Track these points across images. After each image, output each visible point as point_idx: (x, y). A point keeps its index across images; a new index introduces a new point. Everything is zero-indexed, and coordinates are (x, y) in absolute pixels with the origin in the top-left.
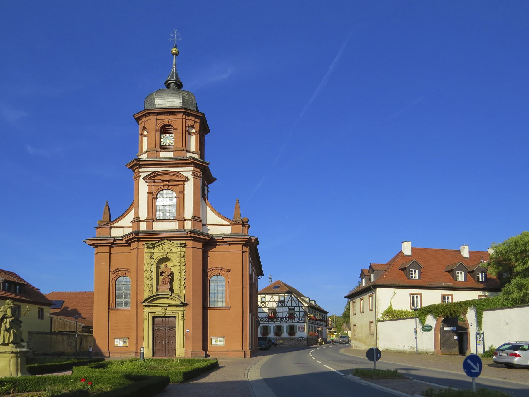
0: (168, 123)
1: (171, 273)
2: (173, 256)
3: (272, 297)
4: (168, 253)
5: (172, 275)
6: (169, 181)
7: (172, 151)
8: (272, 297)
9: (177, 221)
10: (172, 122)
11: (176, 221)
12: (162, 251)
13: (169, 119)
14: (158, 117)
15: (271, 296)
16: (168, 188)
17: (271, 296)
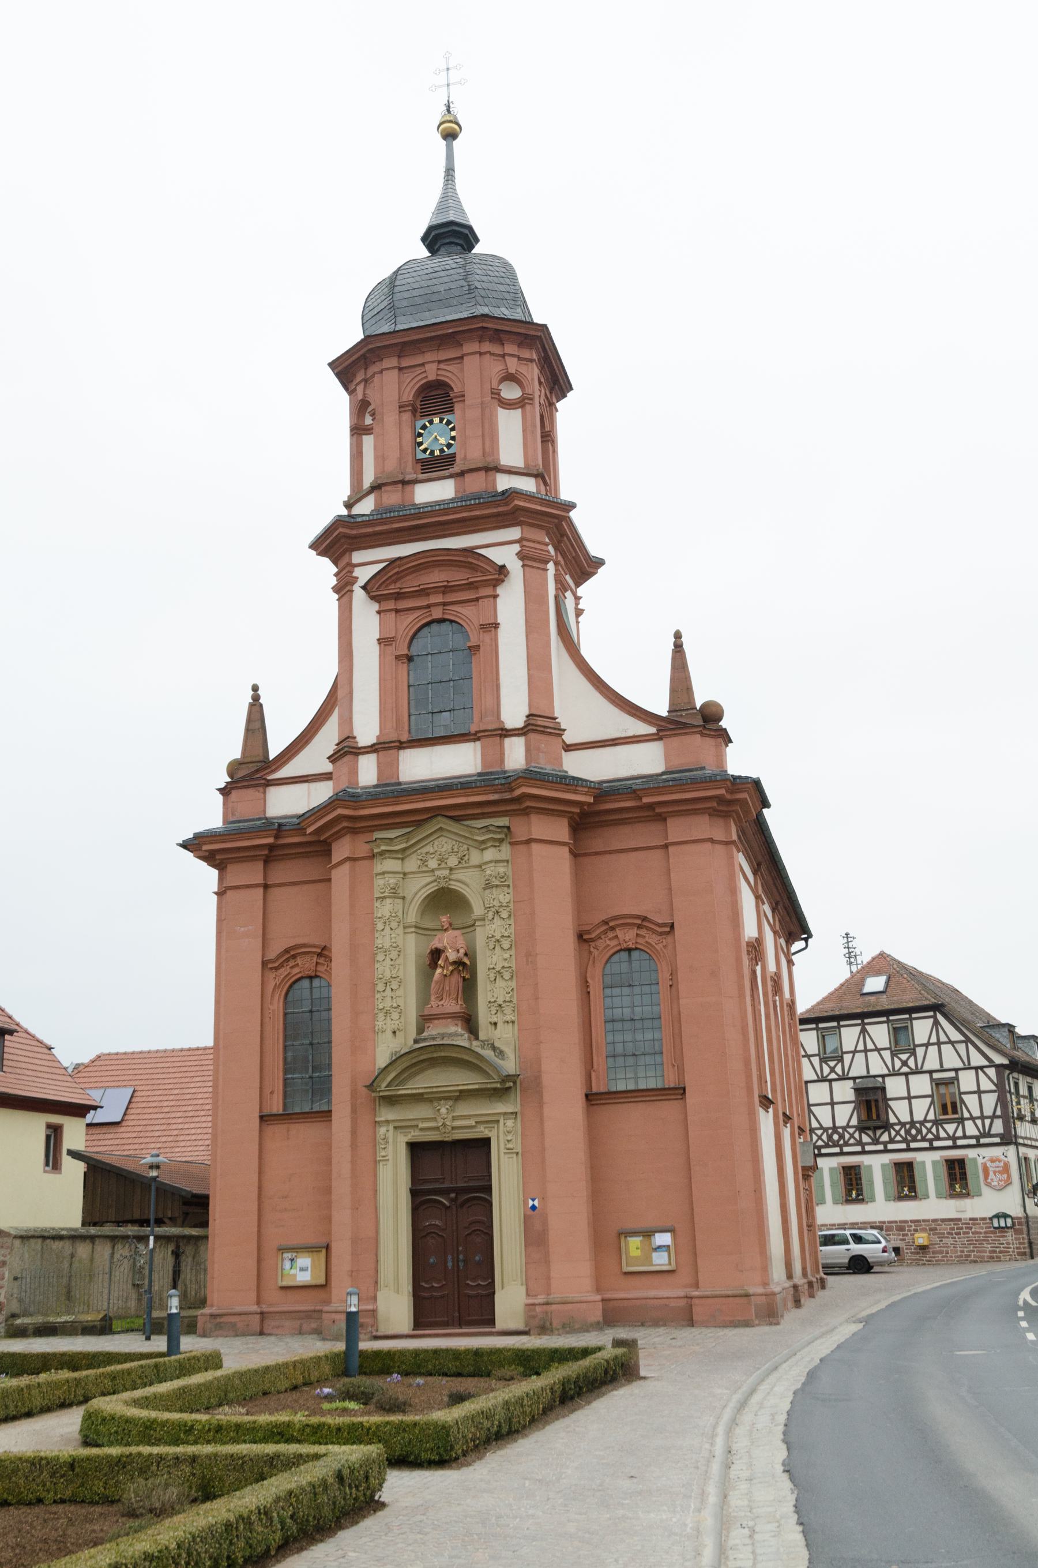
0: (437, 375)
1: (466, 954)
2: (467, 880)
3: (864, 1031)
4: (451, 869)
5: (468, 962)
6: (447, 589)
7: (451, 476)
8: (864, 1031)
9: (478, 739)
10: (450, 374)
11: (474, 740)
12: (433, 864)
13: (439, 362)
14: (406, 362)
15: (859, 1028)
16: (444, 613)
17: (859, 1028)
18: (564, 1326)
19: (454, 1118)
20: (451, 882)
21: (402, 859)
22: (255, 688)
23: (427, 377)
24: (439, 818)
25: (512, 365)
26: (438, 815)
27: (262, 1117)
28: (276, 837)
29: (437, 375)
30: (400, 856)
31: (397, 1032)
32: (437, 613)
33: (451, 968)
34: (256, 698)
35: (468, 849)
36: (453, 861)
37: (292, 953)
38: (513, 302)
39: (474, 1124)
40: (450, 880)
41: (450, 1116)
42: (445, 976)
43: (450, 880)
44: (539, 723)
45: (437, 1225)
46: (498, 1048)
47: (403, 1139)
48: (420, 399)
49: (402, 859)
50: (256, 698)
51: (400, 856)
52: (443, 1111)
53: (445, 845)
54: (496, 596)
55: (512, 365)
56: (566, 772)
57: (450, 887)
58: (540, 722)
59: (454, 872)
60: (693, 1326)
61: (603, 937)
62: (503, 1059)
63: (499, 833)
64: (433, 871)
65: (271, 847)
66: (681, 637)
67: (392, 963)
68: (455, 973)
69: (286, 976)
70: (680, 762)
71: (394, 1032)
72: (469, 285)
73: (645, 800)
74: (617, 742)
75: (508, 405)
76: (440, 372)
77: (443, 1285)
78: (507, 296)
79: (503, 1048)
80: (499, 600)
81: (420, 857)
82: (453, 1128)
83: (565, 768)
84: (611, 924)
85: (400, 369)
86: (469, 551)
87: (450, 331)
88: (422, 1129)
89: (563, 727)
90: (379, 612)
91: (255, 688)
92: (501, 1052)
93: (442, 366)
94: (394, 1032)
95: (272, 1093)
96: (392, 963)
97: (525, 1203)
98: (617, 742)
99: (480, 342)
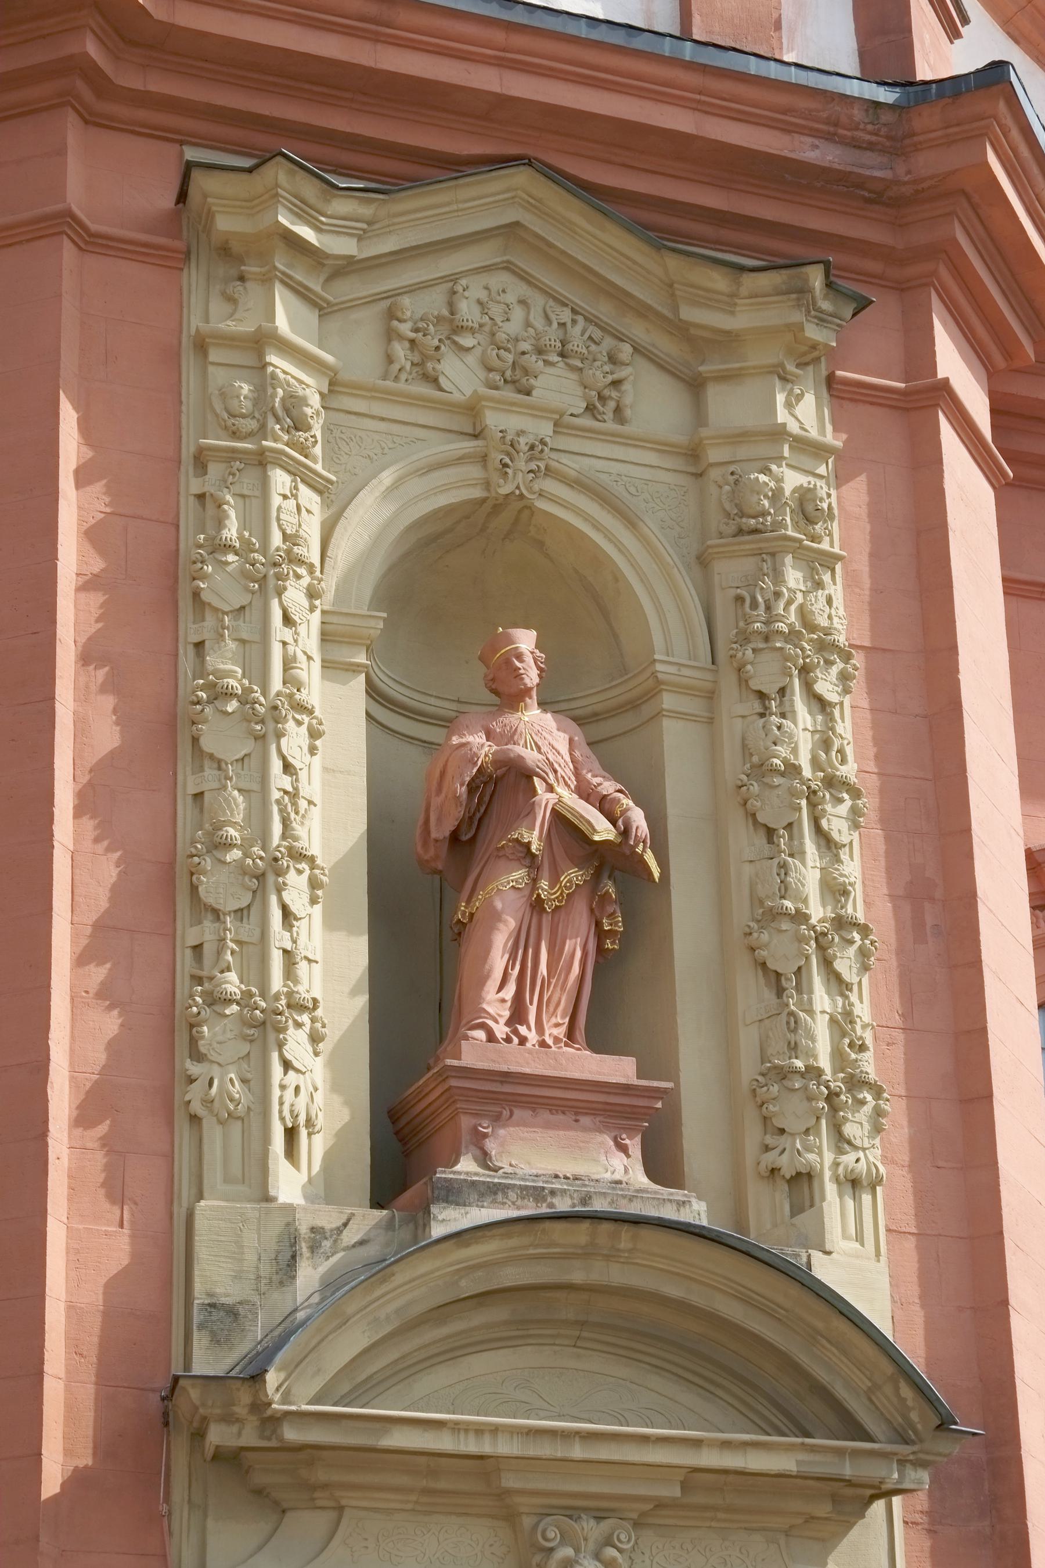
20: (550, 486)
24: (521, 178)
31: (303, 1132)
40: (549, 472)
43: (549, 472)
53: (518, 314)
57: (542, 505)
64: (472, 409)
71: (291, 1134)
94: (291, 1134)
96: (286, 782)
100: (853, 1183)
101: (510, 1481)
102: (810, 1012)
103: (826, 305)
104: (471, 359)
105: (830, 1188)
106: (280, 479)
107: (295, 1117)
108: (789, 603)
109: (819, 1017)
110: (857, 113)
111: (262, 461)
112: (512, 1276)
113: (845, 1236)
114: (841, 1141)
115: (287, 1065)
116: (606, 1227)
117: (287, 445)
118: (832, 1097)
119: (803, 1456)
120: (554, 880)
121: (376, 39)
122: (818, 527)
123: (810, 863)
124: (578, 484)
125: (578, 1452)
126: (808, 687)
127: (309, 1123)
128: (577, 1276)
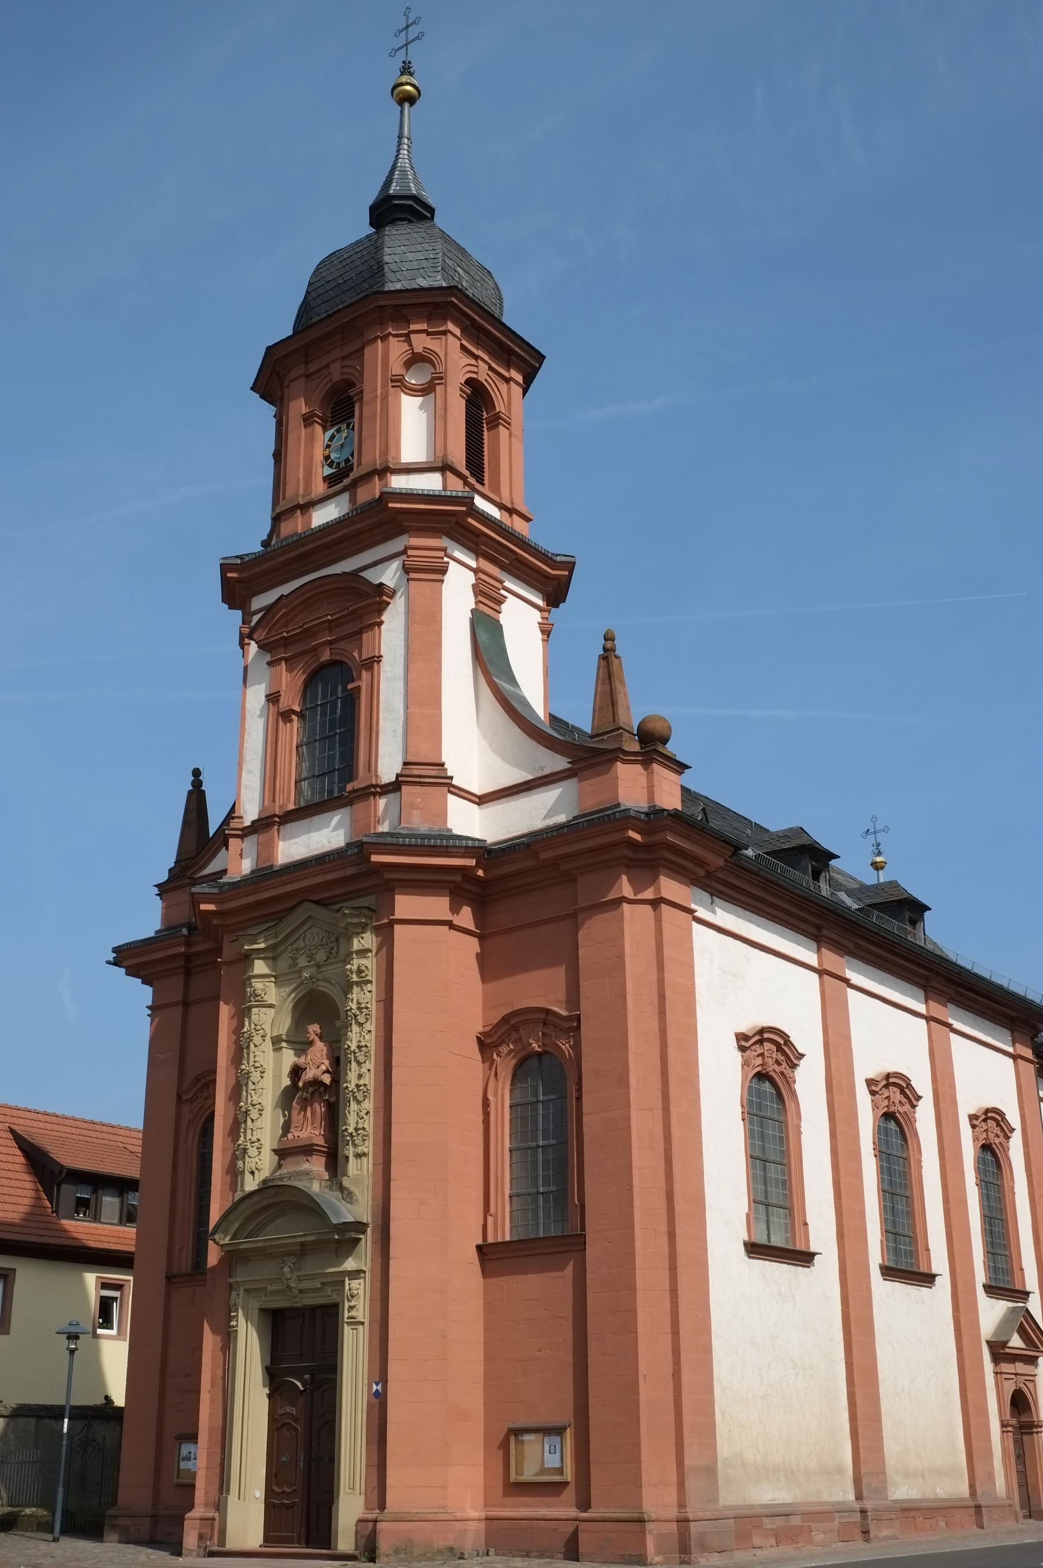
0: (342, 374)
13: (343, 358)
14: (313, 368)
18: (397, 1552)
19: (300, 1279)
20: (320, 983)
21: (274, 959)
22: (197, 773)
23: (331, 380)
25: (421, 342)
26: (303, 901)
27: (168, 1278)
28: (188, 944)
29: (342, 374)
30: (270, 955)
31: (256, 1172)
32: (326, 656)
33: (311, 1090)
34: (197, 784)
35: (337, 940)
36: (321, 956)
37: (203, 1081)
38: (432, 270)
39: (319, 1286)
40: (318, 980)
41: (294, 1276)
42: (306, 1099)
43: (318, 980)
44: (415, 772)
45: (292, 1414)
46: (347, 1189)
47: (255, 1305)
48: (331, 405)
49: (274, 959)
50: (197, 784)
51: (270, 955)
52: (286, 1270)
54: (381, 623)
55: (421, 342)
56: (450, 830)
57: (319, 988)
58: (416, 771)
59: (323, 969)
60: (578, 1560)
61: (506, 1040)
62: (351, 1203)
63: (358, 916)
65: (188, 958)
66: (613, 639)
67: (253, 1087)
68: (316, 1095)
69: (200, 1109)
70: (594, 802)
72: (378, 262)
73: (543, 856)
74: (531, 785)
75: (414, 391)
76: (344, 371)
77: (295, 1490)
78: (425, 264)
79: (352, 1188)
80: (383, 627)
81: (290, 955)
82: (301, 1291)
83: (449, 826)
84: (513, 1022)
85: (307, 377)
86: (355, 575)
87: (346, 320)
88: (271, 1293)
89: (449, 774)
90: (269, 664)
91: (197, 773)
92: (350, 1194)
93: (347, 363)
95: (181, 1249)
96: (253, 1087)
97: (370, 1387)
98: (531, 785)
99: (381, 324)
100: (358, 1156)
101: (268, 1251)
102: (349, 1113)
103: (356, 913)
104: (304, 956)
105: (351, 1158)
106: (255, 1010)
107: (251, 1169)
108: (352, 1000)
109: (352, 1113)
110: (354, 857)
111: (250, 1008)
112: (265, 1203)
113: (358, 1170)
114: (355, 1146)
115: (250, 1157)
116: (276, 1188)
117: (255, 1001)
118: (351, 1135)
119: (316, 1235)
120: (307, 1093)
121: (260, 892)
122: (363, 975)
123: (353, 1070)
124: (323, 980)
125: (274, 1243)
126: (356, 1020)
127: (257, 1169)
128: (277, 1200)
